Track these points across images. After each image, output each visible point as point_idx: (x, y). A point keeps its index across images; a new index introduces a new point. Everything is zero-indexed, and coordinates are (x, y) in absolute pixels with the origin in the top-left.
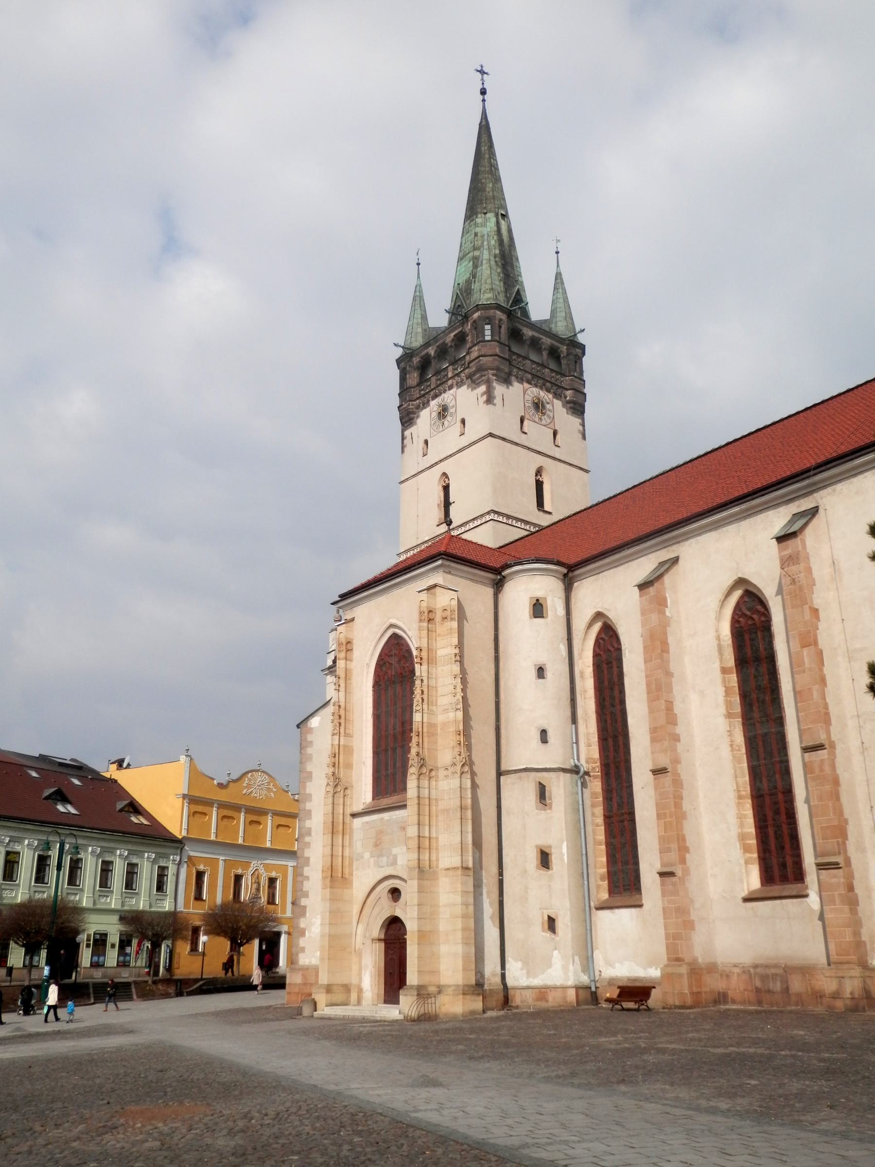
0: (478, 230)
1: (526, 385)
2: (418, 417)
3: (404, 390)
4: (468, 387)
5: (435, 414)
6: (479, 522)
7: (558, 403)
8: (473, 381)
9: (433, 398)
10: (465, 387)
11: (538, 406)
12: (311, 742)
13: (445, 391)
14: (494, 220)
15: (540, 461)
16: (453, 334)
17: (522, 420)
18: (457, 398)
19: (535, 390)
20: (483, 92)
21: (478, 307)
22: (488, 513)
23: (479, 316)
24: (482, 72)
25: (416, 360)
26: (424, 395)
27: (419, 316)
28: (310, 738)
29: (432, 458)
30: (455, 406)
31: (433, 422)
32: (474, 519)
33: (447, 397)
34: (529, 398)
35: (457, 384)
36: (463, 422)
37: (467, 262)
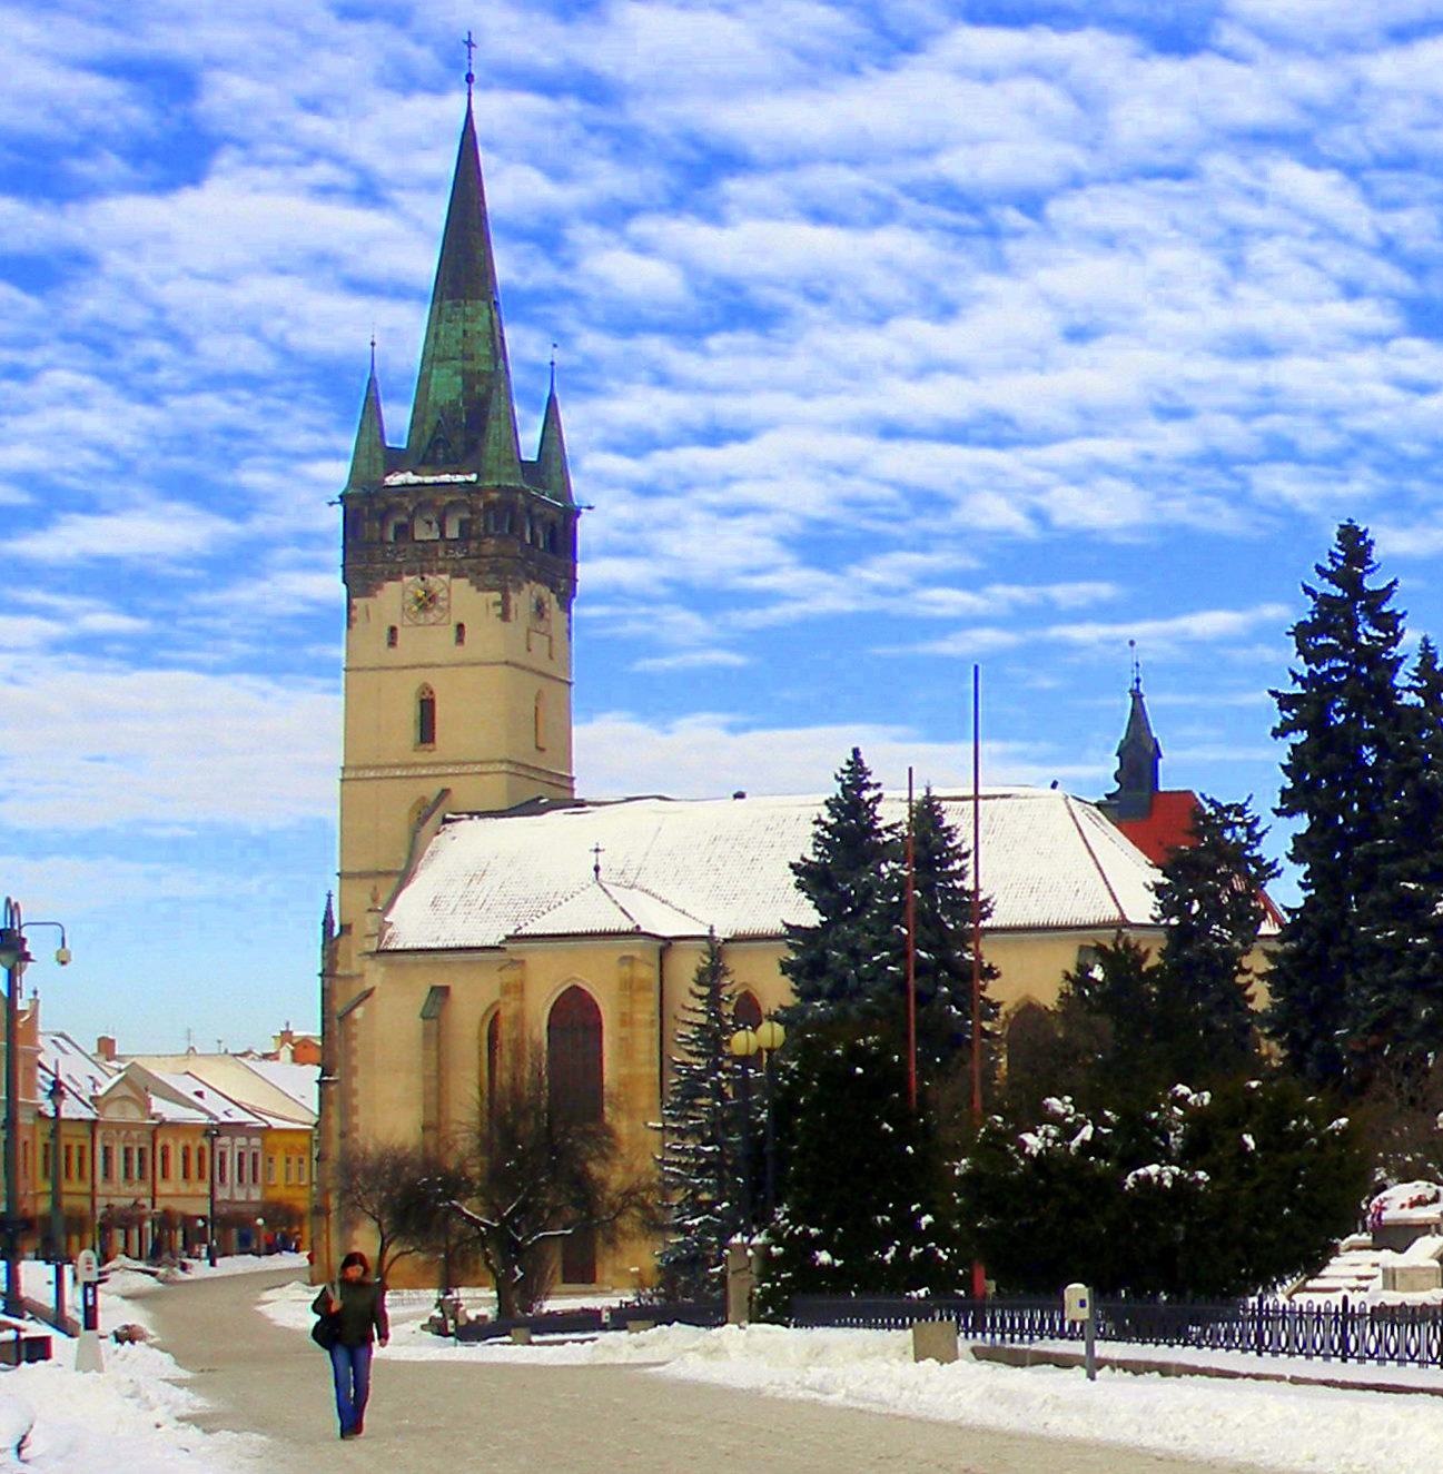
0: (468, 326)
1: (533, 583)
2: (380, 587)
4: (472, 583)
5: (410, 597)
6: (484, 768)
7: (553, 597)
9: (410, 573)
10: (465, 582)
11: (540, 609)
12: (356, 1035)
13: (430, 572)
14: (487, 312)
15: (540, 682)
16: (448, 499)
17: (529, 631)
18: (452, 590)
19: (538, 587)
22: (501, 762)
23: (499, 500)
25: (380, 505)
27: (378, 433)
28: (354, 1029)
30: (448, 599)
31: (407, 606)
32: (481, 762)
33: (431, 579)
34: (534, 601)
35: (454, 570)
36: (460, 627)
37: (450, 372)
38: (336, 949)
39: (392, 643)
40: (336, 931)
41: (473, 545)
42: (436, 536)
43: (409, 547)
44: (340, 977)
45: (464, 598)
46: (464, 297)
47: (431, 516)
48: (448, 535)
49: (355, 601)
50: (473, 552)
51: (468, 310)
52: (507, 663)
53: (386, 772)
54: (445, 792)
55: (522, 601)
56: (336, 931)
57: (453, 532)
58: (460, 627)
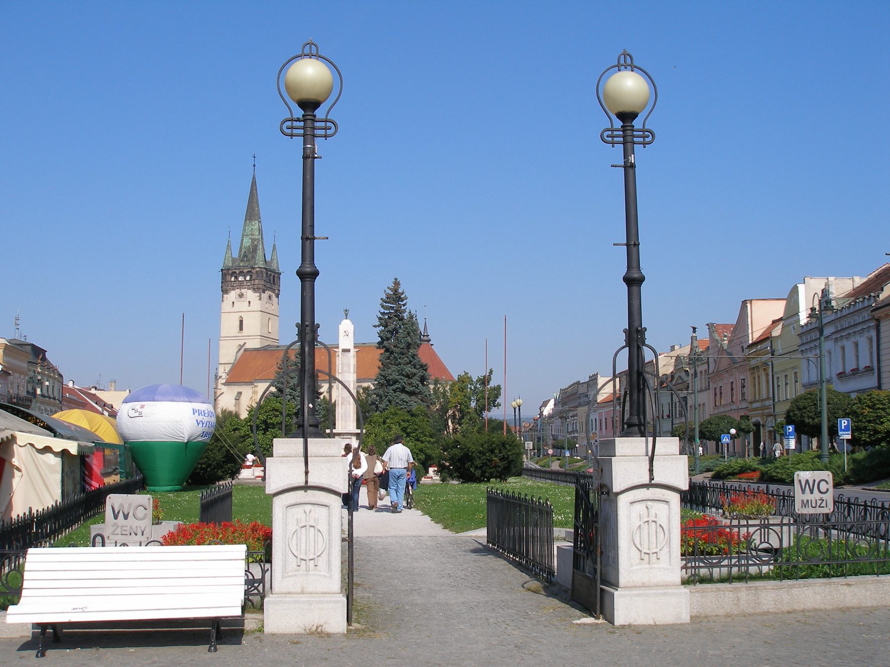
3: (224, 280)
4: (252, 291)
7: (274, 295)
8: (255, 290)
10: (250, 291)
11: (270, 297)
20: (254, 166)
21: (259, 267)
24: (254, 157)
25: (230, 272)
26: (234, 286)
29: (236, 308)
32: (253, 336)
36: (249, 302)
37: (248, 239)
38: (218, 382)
39: (233, 306)
40: (218, 378)
41: (253, 281)
42: (244, 280)
43: (238, 282)
44: (219, 389)
45: (250, 295)
46: (252, 220)
47: (243, 274)
48: (247, 279)
49: (224, 296)
50: (253, 284)
51: (253, 223)
52: (261, 311)
53: (231, 338)
54: (245, 343)
55: (265, 296)
56: (218, 378)
57: (248, 278)
58: (249, 302)
